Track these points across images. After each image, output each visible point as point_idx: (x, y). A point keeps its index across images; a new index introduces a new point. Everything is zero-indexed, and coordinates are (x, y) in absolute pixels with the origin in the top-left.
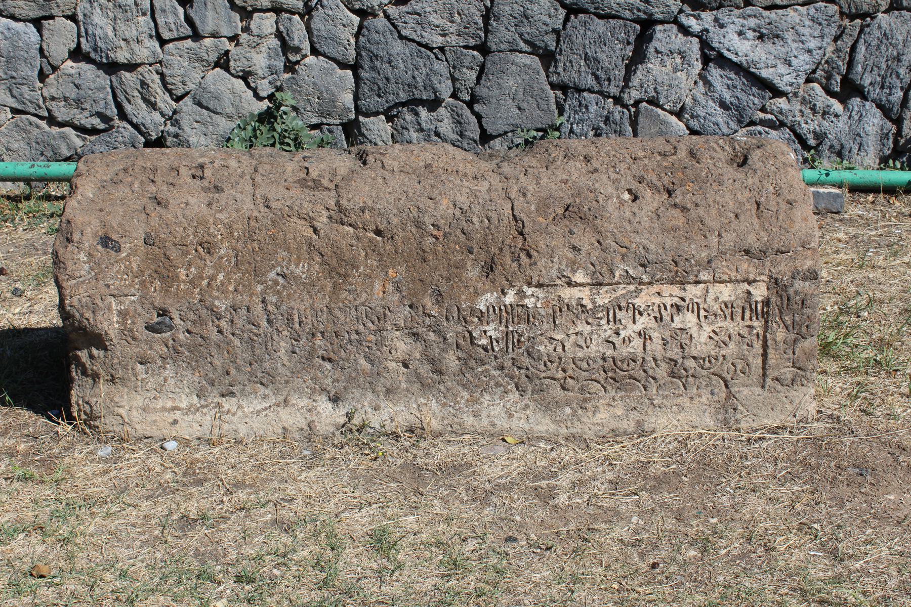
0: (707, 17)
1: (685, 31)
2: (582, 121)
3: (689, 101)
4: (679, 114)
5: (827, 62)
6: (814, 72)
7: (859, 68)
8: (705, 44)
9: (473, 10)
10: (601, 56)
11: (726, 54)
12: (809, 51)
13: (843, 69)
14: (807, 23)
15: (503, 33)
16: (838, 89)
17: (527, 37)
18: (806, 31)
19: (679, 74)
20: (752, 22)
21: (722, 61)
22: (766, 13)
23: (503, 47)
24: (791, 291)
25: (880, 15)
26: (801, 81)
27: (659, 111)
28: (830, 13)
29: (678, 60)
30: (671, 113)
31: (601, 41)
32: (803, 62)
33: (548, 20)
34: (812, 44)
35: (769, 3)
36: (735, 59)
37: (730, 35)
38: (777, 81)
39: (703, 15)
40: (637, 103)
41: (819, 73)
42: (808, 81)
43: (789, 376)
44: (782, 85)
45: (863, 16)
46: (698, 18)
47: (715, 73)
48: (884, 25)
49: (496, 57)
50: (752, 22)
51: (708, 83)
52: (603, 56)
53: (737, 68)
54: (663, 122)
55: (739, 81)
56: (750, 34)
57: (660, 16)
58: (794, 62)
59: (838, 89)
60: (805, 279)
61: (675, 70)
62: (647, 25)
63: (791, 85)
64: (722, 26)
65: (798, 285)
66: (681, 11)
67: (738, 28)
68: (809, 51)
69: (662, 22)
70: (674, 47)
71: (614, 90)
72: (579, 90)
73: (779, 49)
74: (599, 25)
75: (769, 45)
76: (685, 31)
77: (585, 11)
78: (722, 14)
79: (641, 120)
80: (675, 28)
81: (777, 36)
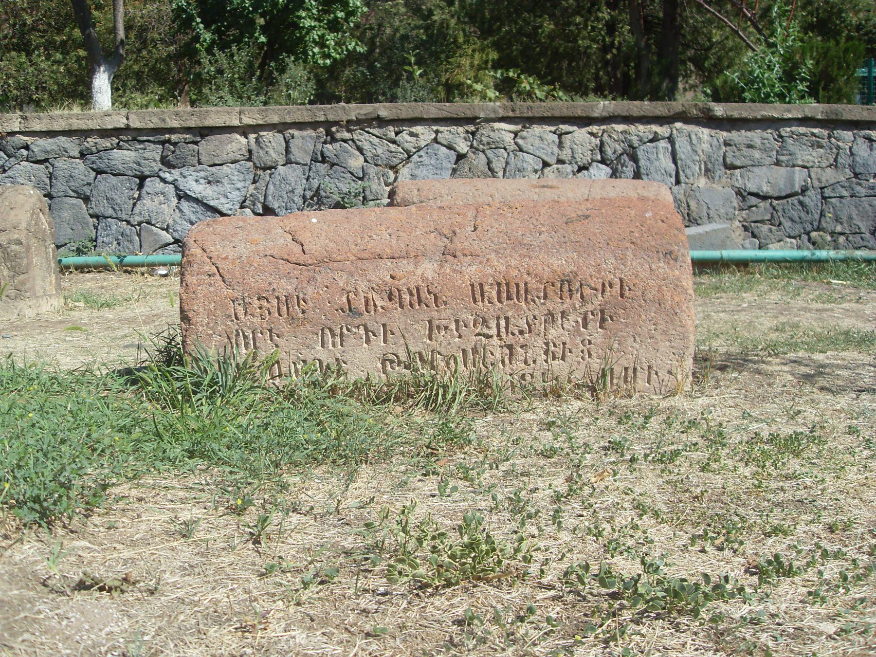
0: (176, 173)
1: (163, 180)
2: (108, 235)
3: (171, 222)
4: (167, 230)
5: (251, 195)
6: (244, 201)
7: (270, 198)
8: (177, 188)
9: (41, 174)
10: (114, 196)
11: (188, 193)
12: (238, 189)
13: (262, 199)
14: (236, 173)
15: (60, 187)
16: (261, 211)
17: (73, 188)
18: (235, 178)
19: (163, 206)
20: (202, 174)
21: (188, 198)
22: (209, 169)
23: (60, 194)
24: (9, 250)
25: (280, 167)
26: (237, 207)
27: (153, 228)
28: (248, 166)
29: (162, 198)
30: (163, 229)
31: (114, 188)
32: (236, 196)
33: (84, 178)
34: (240, 185)
35: (211, 163)
36: (194, 196)
37: (190, 182)
38: (220, 207)
39: (173, 171)
40: (139, 224)
41: (248, 203)
42: (242, 207)
43: (13, 295)
44: (224, 209)
45: (270, 168)
46: (170, 173)
47: (185, 204)
48: (282, 172)
49: (56, 200)
50: (202, 174)
51: (181, 211)
52: (117, 197)
53: (197, 201)
54: (156, 234)
55: (200, 209)
56: (202, 181)
57: (148, 173)
58: (230, 195)
59: (261, 211)
60: (16, 244)
61: (160, 204)
62: (142, 178)
63: (231, 209)
64: (185, 177)
65: (14, 247)
66: (160, 170)
67: (195, 178)
68: (238, 189)
69: (150, 176)
70: (157, 190)
71: (124, 217)
72: (106, 218)
73: (219, 188)
74: (113, 180)
75: (214, 187)
76: (163, 180)
77: (106, 172)
78: (184, 170)
79: (143, 233)
80: (158, 179)
81: (218, 182)
